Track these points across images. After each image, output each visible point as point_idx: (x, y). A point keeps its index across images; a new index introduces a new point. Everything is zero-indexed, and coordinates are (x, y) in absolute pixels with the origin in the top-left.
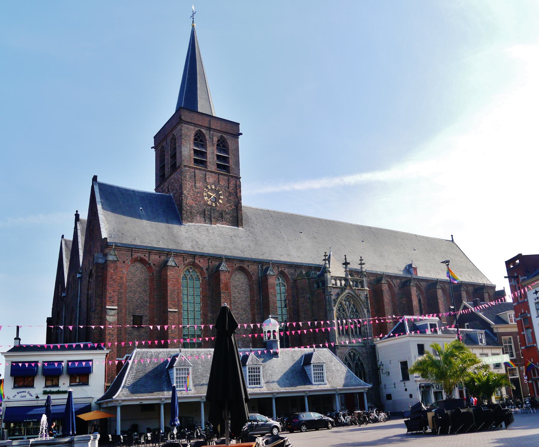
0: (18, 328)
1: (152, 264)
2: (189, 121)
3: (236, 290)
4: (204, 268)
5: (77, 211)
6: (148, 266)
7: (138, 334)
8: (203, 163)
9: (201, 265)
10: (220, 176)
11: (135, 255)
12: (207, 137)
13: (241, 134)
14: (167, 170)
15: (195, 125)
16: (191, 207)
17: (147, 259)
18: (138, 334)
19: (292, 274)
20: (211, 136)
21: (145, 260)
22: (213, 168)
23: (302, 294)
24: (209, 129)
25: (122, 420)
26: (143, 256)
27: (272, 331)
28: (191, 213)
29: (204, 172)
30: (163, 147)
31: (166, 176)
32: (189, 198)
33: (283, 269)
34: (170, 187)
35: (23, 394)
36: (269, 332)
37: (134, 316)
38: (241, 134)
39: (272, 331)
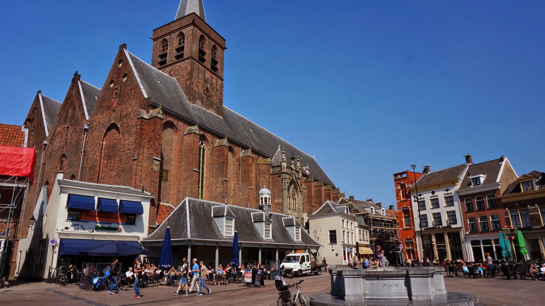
2: (197, 24)
4: (210, 142)
5: (77, 72)
8: (201, 60)
11: (169, 119)
12: (207, 42)
13: (226, 48)
14: (169, 59)
15: (202, 31)
16: (195, 92)
17: (176, 124)
22: (209, 67)
24: (209, 37)
26: (173, 121)
28: (195, 97)
30: (165, 40)
31: (168, 64)
34: (172, 72)
36: (266, 198)
38: (226, 48)
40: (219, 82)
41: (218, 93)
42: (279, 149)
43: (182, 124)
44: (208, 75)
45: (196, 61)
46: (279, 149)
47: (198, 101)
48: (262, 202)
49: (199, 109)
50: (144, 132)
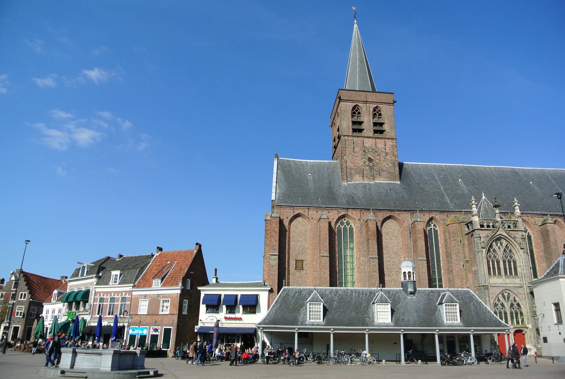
0: (216, 270)
1: (310, 218)
2: (347, 99)
3: (387, 237)
6: (307, 219)
7: (299, 275)
9: (353, 216)
10: (377, 140)
12: (364, 109)
13: (396, 102)
15: (352, 101)
16: (351, 169)
17: (306, 215)
18: (299, 275)
19: (443, 220)
20: (368, 109)
21: (305, 215)
22: (371, 134)
23: (454, 237)
25: (298, 344)
27: (407, 272)
28: (351, 174)
29: (362, 139)
32: (348, 162)
33: (434, 216)
35: (212, 318)
36: (405, 272)
37: (296, 260)
38: (396, 102)
39: (407, 272)
40: (389, 143)
41: (388, 157)
42: (484, 197)
43: (315, 212)
44: (369, 143)
45: (348, 136)
46: (484, 197)
47: (357, 176)
48: (405, 276)
49: (356, 186)
50: (269, 232)
